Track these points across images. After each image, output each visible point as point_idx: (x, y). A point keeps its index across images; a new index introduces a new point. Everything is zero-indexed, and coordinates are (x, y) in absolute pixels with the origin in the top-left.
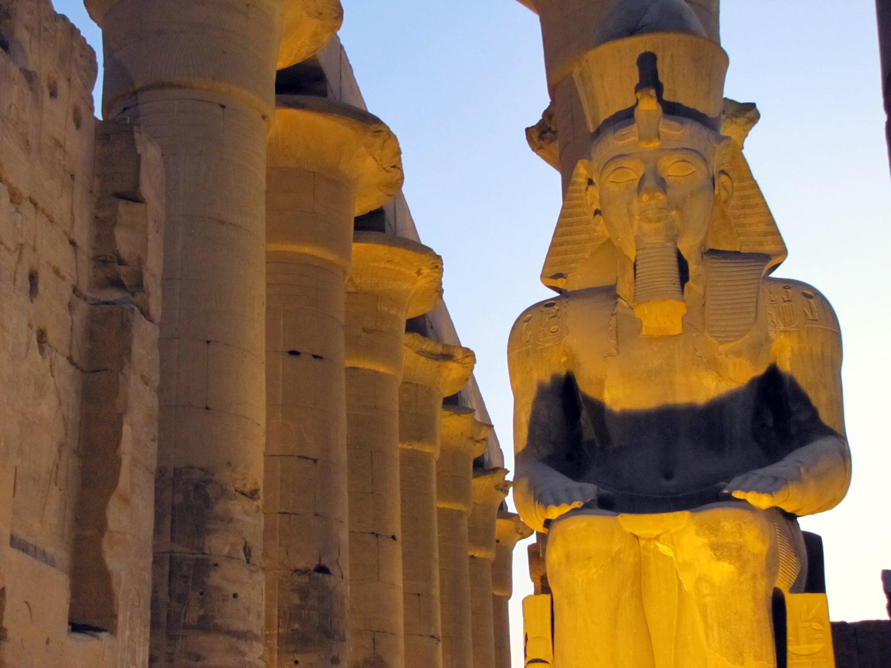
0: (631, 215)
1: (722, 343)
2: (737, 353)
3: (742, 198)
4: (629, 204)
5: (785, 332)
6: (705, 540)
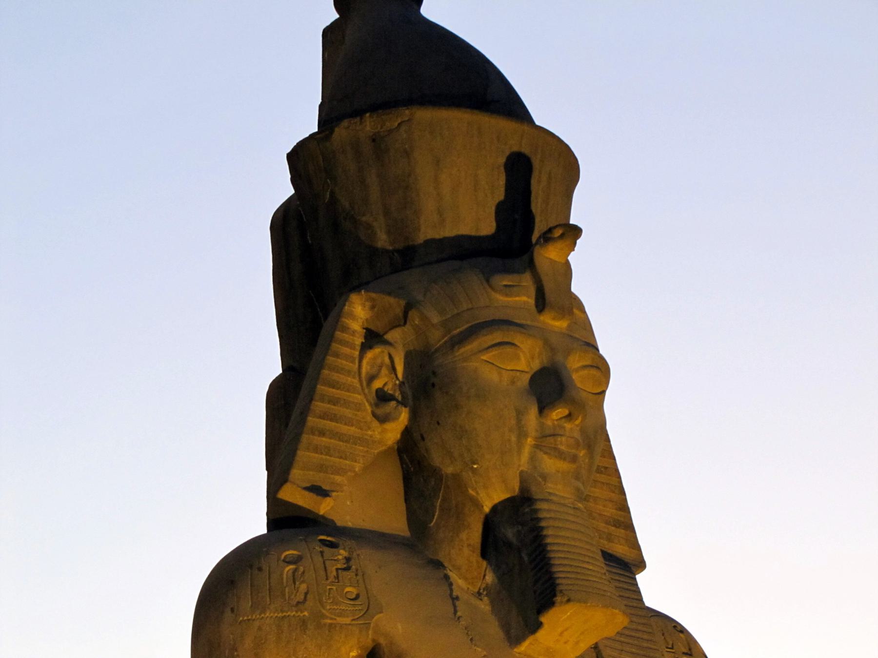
0: (522, 434)
4: (520, 414)
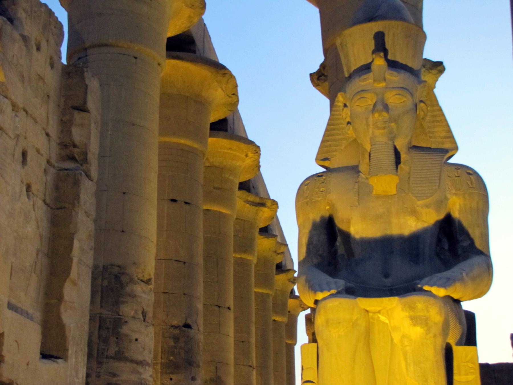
0: (368, 125)
1: (419, 200)
2: (427, 206)
3: (433, 116)
4: (367, 119)
5: (456, 194)
6: (407, 314)
